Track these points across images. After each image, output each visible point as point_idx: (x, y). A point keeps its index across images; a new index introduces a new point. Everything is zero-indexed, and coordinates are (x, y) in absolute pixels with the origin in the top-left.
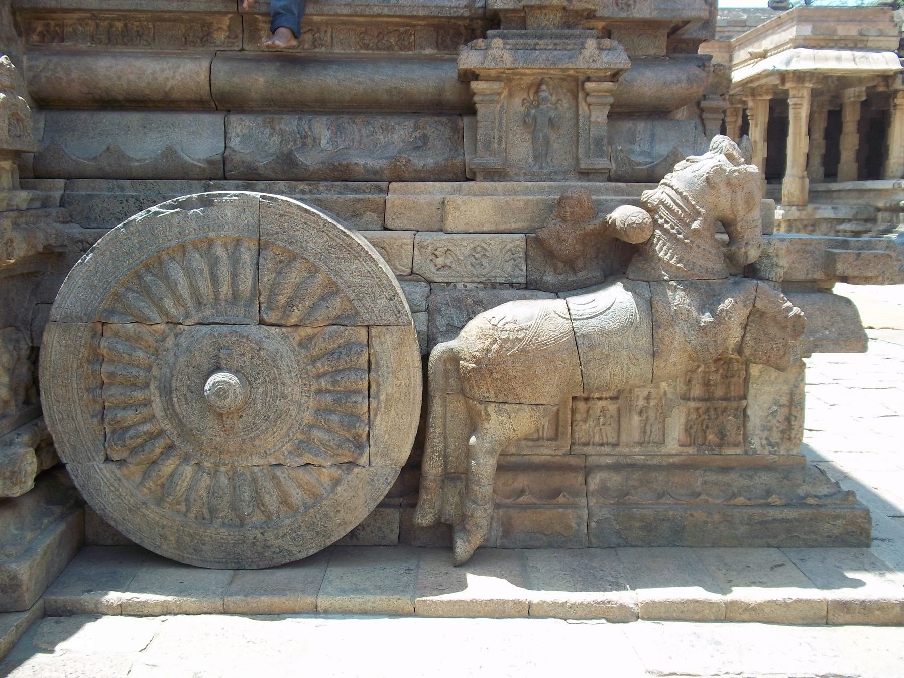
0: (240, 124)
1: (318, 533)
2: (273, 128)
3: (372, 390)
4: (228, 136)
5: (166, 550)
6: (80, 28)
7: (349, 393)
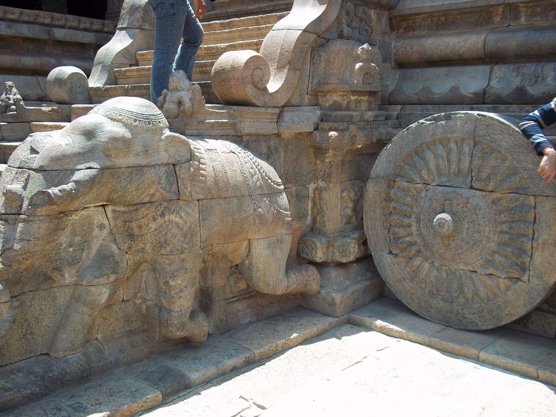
0: (500, 70)
1: (494, 317)
2: (519, 72)
3: (535, 236)
4: (491, 78)
5: (413, 307)
6: (423, 23)
7: (520, 235)
